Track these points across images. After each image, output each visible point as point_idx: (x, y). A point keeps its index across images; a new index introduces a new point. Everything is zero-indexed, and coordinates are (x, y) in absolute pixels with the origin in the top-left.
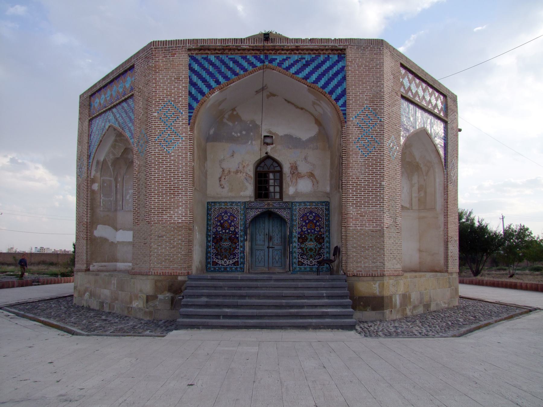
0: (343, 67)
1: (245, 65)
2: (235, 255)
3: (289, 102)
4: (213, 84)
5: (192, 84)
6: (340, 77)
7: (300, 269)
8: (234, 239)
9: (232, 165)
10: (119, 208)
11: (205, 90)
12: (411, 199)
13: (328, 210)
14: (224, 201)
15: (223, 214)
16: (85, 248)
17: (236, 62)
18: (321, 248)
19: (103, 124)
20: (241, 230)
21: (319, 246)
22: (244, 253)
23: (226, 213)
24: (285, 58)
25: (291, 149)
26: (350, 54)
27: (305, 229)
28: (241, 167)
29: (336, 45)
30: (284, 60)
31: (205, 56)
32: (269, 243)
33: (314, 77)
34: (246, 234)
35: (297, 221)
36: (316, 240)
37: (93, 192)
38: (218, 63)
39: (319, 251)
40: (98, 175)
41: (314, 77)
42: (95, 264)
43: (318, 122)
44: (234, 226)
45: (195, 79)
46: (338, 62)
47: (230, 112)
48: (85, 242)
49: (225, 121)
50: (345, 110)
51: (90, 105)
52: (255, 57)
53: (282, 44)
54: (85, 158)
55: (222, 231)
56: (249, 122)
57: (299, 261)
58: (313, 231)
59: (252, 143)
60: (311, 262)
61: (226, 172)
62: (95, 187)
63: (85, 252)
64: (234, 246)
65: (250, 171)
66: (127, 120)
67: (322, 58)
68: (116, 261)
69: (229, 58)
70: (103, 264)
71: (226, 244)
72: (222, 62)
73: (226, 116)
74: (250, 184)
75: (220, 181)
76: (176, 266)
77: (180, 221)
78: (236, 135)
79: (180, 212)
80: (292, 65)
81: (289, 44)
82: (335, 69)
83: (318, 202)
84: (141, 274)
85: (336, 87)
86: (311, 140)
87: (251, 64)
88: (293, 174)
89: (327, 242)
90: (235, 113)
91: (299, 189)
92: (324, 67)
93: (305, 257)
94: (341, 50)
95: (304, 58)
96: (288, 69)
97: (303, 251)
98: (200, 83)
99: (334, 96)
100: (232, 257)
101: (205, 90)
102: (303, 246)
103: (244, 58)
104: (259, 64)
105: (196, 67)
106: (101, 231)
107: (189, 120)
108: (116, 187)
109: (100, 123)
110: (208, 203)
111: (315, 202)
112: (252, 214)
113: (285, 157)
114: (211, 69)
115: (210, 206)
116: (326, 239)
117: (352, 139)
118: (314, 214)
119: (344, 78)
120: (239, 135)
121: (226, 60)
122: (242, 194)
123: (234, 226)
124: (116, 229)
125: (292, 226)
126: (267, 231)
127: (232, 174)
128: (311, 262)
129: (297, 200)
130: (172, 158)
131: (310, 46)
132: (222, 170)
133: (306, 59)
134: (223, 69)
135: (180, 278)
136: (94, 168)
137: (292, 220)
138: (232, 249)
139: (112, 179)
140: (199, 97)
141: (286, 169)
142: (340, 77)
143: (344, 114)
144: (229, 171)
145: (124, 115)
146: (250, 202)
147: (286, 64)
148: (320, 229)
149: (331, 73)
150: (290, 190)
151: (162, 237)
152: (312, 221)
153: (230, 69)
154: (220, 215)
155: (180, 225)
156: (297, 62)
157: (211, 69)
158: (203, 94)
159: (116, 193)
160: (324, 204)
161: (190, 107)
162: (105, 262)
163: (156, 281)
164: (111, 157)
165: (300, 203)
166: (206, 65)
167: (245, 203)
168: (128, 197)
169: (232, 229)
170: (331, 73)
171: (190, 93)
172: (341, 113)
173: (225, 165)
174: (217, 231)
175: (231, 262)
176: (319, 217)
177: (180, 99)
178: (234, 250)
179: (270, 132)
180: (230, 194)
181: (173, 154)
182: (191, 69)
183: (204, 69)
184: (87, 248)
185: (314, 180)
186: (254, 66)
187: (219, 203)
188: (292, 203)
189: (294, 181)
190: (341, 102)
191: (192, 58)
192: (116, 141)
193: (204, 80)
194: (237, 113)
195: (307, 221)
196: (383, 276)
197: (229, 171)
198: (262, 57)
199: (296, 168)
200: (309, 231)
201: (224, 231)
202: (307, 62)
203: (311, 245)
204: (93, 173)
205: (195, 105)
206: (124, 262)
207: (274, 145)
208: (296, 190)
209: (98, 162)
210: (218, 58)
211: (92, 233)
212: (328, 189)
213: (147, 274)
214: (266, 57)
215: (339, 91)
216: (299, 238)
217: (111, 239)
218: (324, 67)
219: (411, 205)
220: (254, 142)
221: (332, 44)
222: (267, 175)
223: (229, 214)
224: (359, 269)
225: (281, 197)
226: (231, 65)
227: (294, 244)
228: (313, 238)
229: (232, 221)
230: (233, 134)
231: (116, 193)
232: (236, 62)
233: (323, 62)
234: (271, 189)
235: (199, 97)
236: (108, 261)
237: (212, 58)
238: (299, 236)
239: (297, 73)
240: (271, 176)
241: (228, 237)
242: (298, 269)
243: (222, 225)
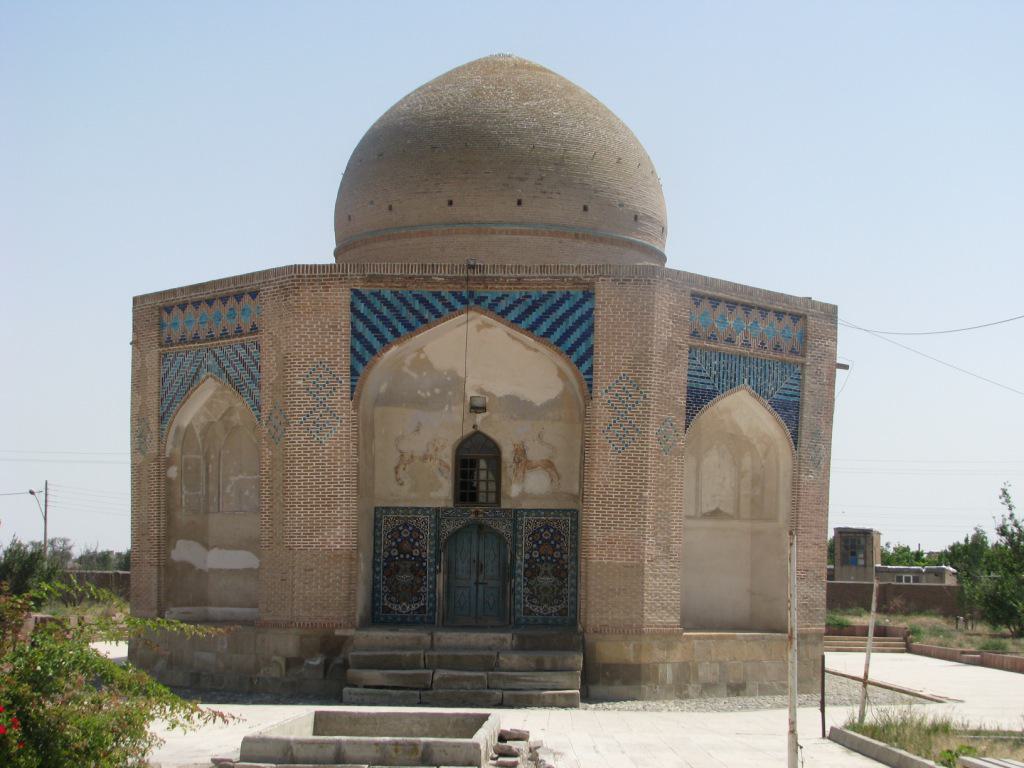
0: (591, 310)
1: (439, 306)
2: (419, 596)
4: (388, 335)
5: (356, 335)
7: (528, 620)
8: (418, 570)
9: (416, 446)
10: (211, 509)
11: (376, 344)
12: (738, 501)
13: (576, 523)
14: (402, 505)
15: (401, 528)
16: (155, 581)
17: (423, 301)
18: (561, 588)
19: (193, 369)
20: (430, 555)
21: (559, 583)
22: (434, 593)
23: (406, 525)
24: (500, 296)
25: (515, 419)
26: (603, 291)
27: (536, 555)
28: (432, 451)
29: (581, 275)
30: (499, 299)
32: (478, 576)
33: (544, 327)
34: (438, 561)
35: (524, 542)
36: (553, 574)
37: (169, 481)
38: (396, 303)
39: (558, 592)
40: (178, 450)
42: (172, 609)
44: (420, 548)
45: (360, 326)
46: (582, 301)
47: (414, 355)
48: (155, 570)
49: (405, 369)
50: (591, 380)
51: (161, 325)
52: (454, 294)
53: (496, 275)
54: (153, 420)
55: (398, 556)
56: (445, 373)
57: (525, 608)
58: (549, 558)
59: (450, 408)
60: (546, 610)
61: (407, 457)
62: (173, 472)
63: (154, 587)
64: (419, 582)
65: (447, 456)
66: (245, 376)
67: (557, 297)
69: (414, 295)
70: (186, 609)
71: (405, 578)
72: (402, 299)
73: (408, 361)
74: (446, 478)
75: (397, 473)
76: (331, 614)
77: (338, 547)
78: (423, 395)
79: (338, 534)
81: (506, 275)
82: (578, 313)
83: (558, 510)
84: (276, 625)
85: (578, 343)
86: (551, 405)
88: (517, 461)
89: (572, 577)
90: (422, 356)
91: (526, 488)
92: (560, 312)
93: (535, 601)
94: (588, 284)
95: (530, 297)
97: (533, 591)
98: (368, 335)
99: (575, 357)
100: (414, 599)
101: (376, 344)
102: (532, 582)
104: (459, 306)
105: (362, 308)
106: (184, 551)
107: (352, 392)
108: (207, 469)
110: (376, 509)
111: (553, 510)
112: (449, 527)
113: (505, 434)
114: (385, 311)
115: (379, 515)
116: (571, 572)
118: (552, 531)
119: (591, 329)
120: (429, 394)
121: (409, 297)
122: (432, 494)
123: (420, 548)
124: (207, 547)
125: (515, 549)
126: (474, 556)
127: (417, 461)
128: (546, 610)
129: (525, 505)
130: (326, 451)
132: (399, 454)
133: (533, 298)
134: (405, 312)
135: (338, 632)
136: (171, 438)
137: (515, 540)
138: (416, 588)
139: (200, 457)
141: (507, 454)
142: (584, 327)
143: (590, 386)
144: (412, 457)
146: (446, 509)
147: (503, 305)
148: (562, 554)
149: (572, 320)
150: (514, 490)
151: (312, 570)
152: (549, 541)
153: (413, 311)
154: (396, 530)
155: (338, 553)
156: (519, 301)
157: (385, 311)
158: (373, 352)
159: (207, 482)
160: (568, 513)
161: (354, 372)
162: (188, 605)
164: (203, 419)
165: (529, 511)
166: (378, 304)
167: (437, 510)
168: (228, 490)
169: (416, 552)
170: (572, 320)
171: (353, 350)
172: (586, 383)
173: (405, 446)
174: (390, 556)
175: (414, 608)
176: (560, 534)
177: (338, 359)
178: (418, 589)
179: (482, 391)
180: (413, 495)
181: (327, 445)
182: (354, 310)
183: (375, 312)
184: (159, 582)
185: (553, 473)
186: (452, 309)
187: (395, 509)
188: (516, 511)
189: (520, 474)
190: (585, 367)
191: (356, 293)
192: (214, 396)
193: (374, 330)
194: (426, 357)
195: (540, 542)
196: (640, 632)
197: (412, 457)
199: (524, 452)
200: (543, 558)
201: (402, 556)
202: (533, 302)
203: (546, 580)
204: (169, 447)
205: (360, 368)
206: (222, 605)
207: (487, 413)
208: (524, 488)
209: (178, 430)
210: (395, 293)
211: (168, 555)
214: (471, 294)
215: (582, 349)
216: (526, 570)
217: (199, 565)
218: (560, 312)
219: (738, 509)
220: (453, 408)
221: (575, 274)
222: (476, 462)
223: (410, 528)
224: (605, 622)
225: (498, 501)
226: (417, 306)
227: (518, 579)
228: (549, 569)
229: (415, 540)
230: (419, 392)
231: (207, 482)
232: (423, 301)
233: (561, 302)
234: (482, 487)
235: (367, 355)
236: (194, 605)
237: (388, 295)
238: (526, 566)
239: (518, 320)
240: (483, 464)
241: (408, 566)
242: (523, 620)
243: (398, 547)
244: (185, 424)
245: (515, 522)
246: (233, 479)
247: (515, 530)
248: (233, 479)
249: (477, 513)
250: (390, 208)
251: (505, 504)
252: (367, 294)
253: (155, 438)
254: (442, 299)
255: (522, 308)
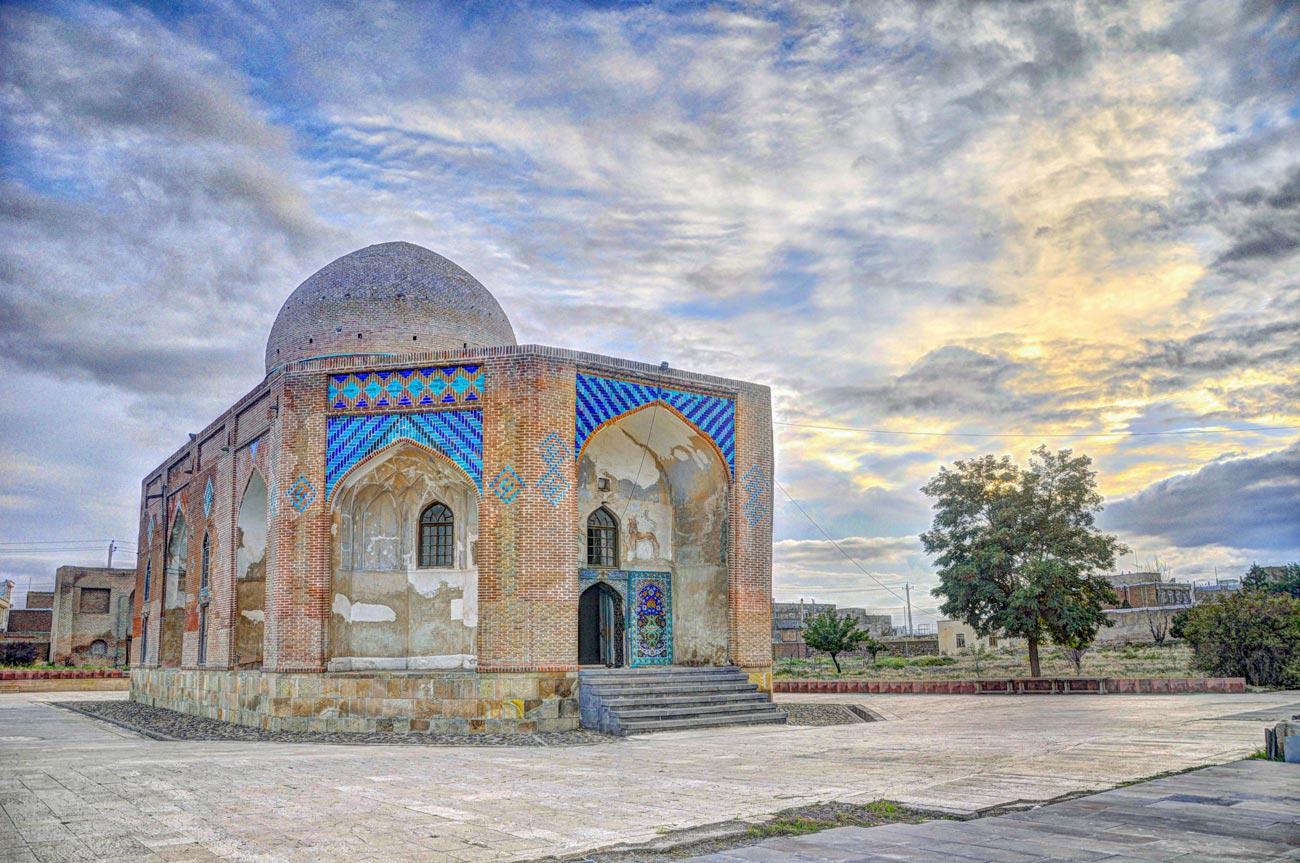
1: (637, 396)
3: (626, 434)
6: (729, 427)
13: (669, 583)
17: (626, 391)
19: (378, 434)
26: (741, 400)
30: (677, 397)
31: (593, 377)
33: (705, 423)
35: (637, 598)
41: (705, 423)
43: (660, 466)
46: (728, 407)
48: (318, 622)
52: (648, 388)
67: (713, 400)
68: (352, 654)
72: (612, 387)
80: (685, 405)
82: (725, 416)
86: (652, 489)
87: (644, 397)
88: (631, 533)
96: (680, 409)
98: (587, 413)
99: (723, 450)
102: (643, 630)
103: (637, 388)
104: (651, 399)
109: (369, 426)
113: (625, 510)
114: (600, 395)
117: (742, 504)
121: (617, 386)
124: (352, 602)
129: (637, 569)
131: (704, 384)
140: (586, 432)
141: (624, 527)
142: (729, 427)
145: (448, 432)
147: (679, 403)
150: (627, 556)
152: (652, 597)
153: (621, 399)
156: (690, 401)
157: (600, 395)
158: (590, 428)
161: (577, 446)
163: (541, 680)
168: (369, 549)
172: (730, 471)
179: (607, 474)
182: (579, 394)
183: (593, 395)
186: (647, 401)
190: (730, 457)
191: (579, 377)
193: (591, 410)
198: (655, 389)
199: (636, 527)
205: (581, 442)
212: (670, 556)
213: (527, 671)
214: (659, 390)
215: (728, 444)
222: (602, 534)
226: (623, 394)
232: (626, 391)
233: (715, 405)
235: (586, 432)
237: (601, 381)
244: (350, 485)
245: (629, 581)
246: (373, 539)
247: (630, 588)
248: (373, 539)
249: (603, 574)
250: (360, 335)
251: (623, 567)
252: (587, 379)
253: (319, 496)
254: (640, 392)
255: (691, 407)
